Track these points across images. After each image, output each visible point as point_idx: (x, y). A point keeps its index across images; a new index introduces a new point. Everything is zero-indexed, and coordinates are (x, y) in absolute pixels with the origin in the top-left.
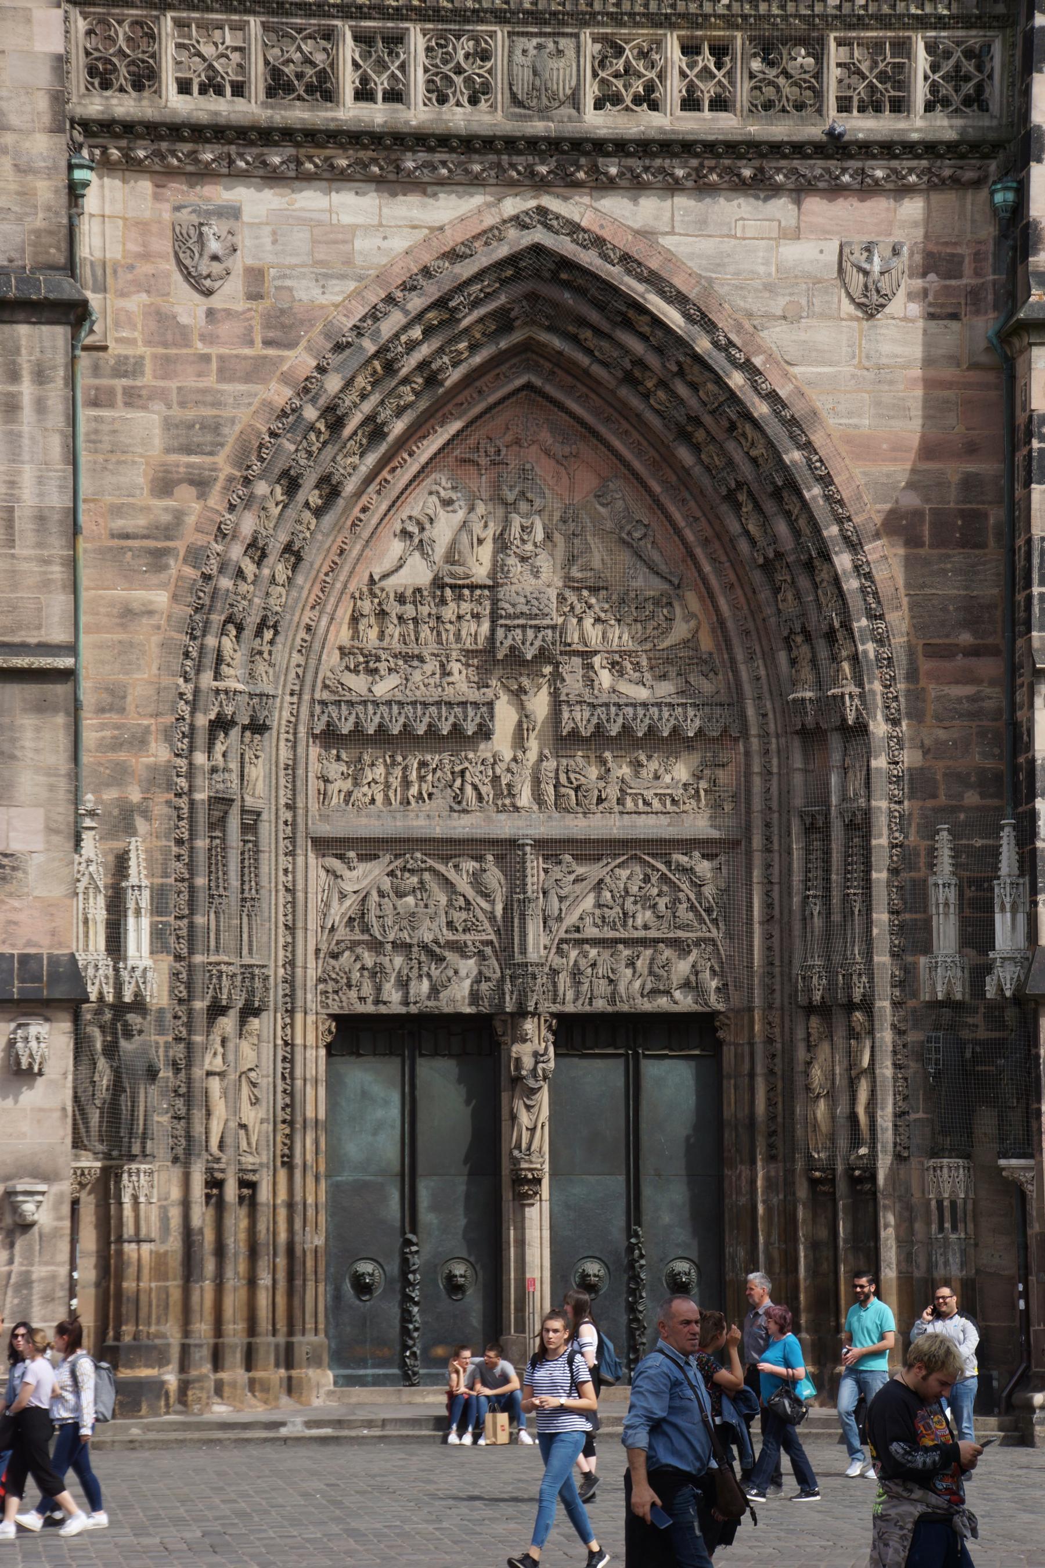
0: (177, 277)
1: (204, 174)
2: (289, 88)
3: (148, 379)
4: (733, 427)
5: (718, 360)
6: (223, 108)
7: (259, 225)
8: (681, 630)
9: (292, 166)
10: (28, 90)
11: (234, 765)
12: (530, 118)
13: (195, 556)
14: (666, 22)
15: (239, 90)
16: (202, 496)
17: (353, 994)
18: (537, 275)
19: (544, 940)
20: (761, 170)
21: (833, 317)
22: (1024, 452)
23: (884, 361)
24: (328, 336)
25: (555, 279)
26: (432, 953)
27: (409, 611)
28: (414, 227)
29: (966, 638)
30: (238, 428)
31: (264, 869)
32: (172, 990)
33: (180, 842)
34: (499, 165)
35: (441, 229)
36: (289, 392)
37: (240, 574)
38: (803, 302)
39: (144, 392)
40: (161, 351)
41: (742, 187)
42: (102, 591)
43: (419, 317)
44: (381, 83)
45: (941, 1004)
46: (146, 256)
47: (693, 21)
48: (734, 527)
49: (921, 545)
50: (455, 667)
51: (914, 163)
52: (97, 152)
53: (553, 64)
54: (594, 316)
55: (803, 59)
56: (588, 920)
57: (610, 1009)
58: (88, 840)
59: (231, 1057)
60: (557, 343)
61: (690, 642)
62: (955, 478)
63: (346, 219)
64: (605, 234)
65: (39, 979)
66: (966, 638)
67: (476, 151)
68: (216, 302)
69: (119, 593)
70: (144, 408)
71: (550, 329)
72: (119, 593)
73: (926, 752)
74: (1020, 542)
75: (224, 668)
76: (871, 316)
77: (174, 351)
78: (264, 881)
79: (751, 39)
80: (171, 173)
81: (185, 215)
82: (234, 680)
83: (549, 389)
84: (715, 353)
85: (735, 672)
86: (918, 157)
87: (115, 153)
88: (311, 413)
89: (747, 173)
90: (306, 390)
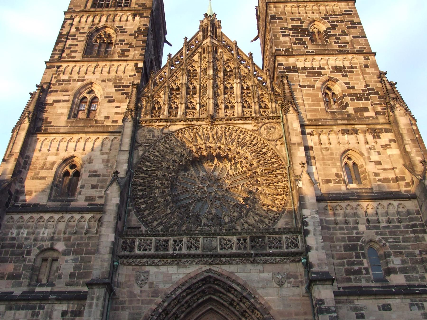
0: (135, 285)
2: (160, 249)
3: (127, 305)
4: (253, 312)
5: (248, 297)
7: (153, 274)
10: (106, 247)
20: (255, 259)
21: (271, 287)
30: (144, 314)
34: (201, 260)
35: (190, 273)
36: (156, 306)
44: (177, 248)
46: (129, 281)
51: (285, 257)
63: (170, 272)
64: (224, 273)
67: (197, 258)
68: (143, 289)
70: (125, 310)
71: (214, 295)
80: (136, 265)
83: (215, 309)
86: (286, 256)
88: (160, 310)
89: (252, 260)
90: (159, 306)
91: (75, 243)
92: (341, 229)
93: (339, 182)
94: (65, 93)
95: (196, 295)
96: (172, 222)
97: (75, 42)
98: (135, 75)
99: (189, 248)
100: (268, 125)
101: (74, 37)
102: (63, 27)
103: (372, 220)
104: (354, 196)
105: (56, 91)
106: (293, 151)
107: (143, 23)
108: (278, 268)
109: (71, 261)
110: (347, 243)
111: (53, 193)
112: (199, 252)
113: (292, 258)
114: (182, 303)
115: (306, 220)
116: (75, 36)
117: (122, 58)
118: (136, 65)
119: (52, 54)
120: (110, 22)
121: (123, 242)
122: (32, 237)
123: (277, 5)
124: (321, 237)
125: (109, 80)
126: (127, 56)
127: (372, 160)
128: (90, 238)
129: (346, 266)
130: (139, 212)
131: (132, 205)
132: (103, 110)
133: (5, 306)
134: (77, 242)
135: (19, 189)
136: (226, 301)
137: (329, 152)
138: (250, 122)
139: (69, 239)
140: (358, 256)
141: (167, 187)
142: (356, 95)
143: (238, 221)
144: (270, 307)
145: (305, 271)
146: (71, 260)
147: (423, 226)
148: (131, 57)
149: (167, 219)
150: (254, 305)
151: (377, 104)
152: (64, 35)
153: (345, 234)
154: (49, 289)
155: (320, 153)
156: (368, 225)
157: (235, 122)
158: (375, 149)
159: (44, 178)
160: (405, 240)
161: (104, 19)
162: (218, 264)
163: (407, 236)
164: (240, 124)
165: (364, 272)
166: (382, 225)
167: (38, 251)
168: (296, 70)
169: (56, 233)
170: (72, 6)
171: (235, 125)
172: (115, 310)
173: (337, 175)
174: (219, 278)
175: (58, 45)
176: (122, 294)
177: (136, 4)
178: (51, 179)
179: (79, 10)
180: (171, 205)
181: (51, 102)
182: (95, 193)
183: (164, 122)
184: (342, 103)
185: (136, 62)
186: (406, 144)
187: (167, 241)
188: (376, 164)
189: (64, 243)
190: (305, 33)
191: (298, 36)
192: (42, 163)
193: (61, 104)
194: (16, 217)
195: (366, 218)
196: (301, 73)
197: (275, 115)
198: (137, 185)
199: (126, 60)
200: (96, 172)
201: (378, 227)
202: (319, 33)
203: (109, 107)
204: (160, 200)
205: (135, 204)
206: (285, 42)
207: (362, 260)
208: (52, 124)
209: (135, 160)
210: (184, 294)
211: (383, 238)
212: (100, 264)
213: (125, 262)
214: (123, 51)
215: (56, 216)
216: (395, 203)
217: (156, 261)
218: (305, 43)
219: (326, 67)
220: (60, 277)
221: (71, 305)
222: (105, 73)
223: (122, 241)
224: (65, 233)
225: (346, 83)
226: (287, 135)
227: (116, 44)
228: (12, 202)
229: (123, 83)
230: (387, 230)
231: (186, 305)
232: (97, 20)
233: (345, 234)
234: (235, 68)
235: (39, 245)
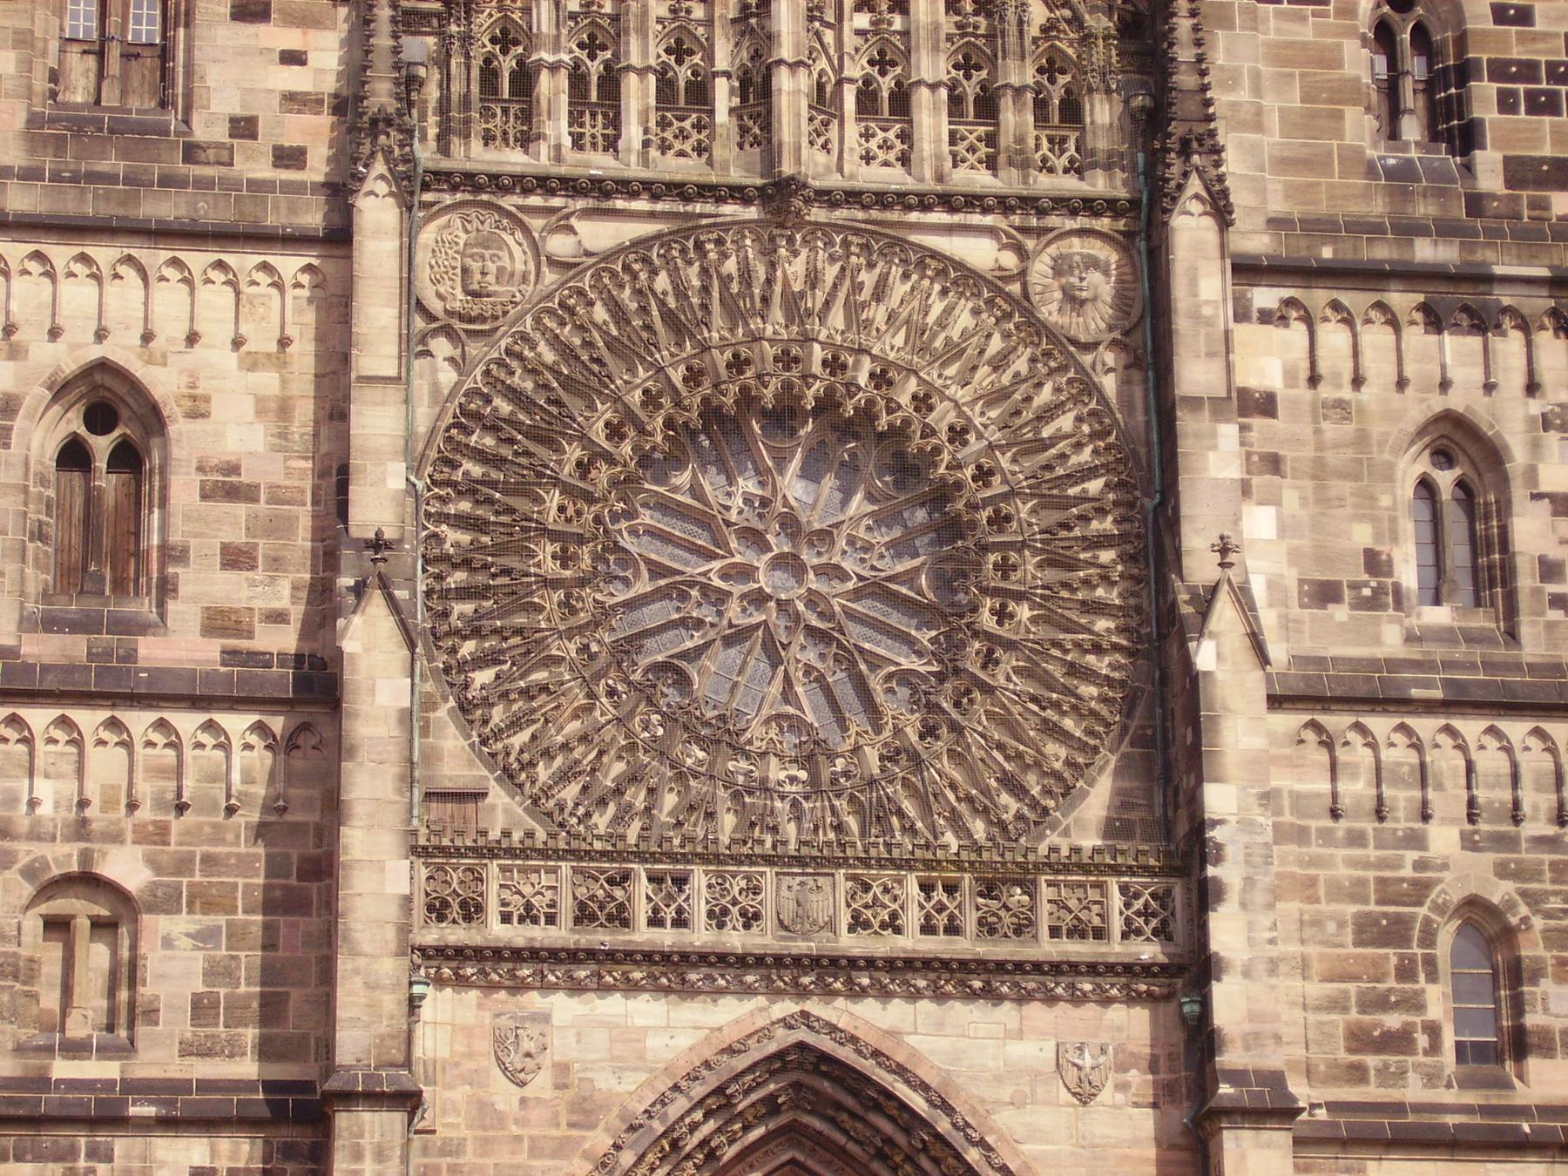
0: (497, 1071)
1: (518, 987)
2: (593, 917)
5: (957, 1139)
6: (541, 935)
7: (566, 1027)
9: (595, 979)
12: (795, 940)
14: (908, 864)
15: (551, 919)
18: (800, 1066)
20: (988, 983)
23: (1097, 1141)
24: (622, 1118)
25: (816, 1071)
28: (697, 1028)
34: (769, 978)
35: (720, 1029)
38: (1028, 1090)
39: (465, 1169)
40: (481, 1133)
43: (701, 1102)
44: (669, 914)
46: (470, 1055)
47: (929, 865)
51: (1115, 980)
52: (432, 971)
53: (813, 897)
54: (849, 1101)
55: (1018, 896)
60: (817, 1124)
63: (639, 1022)
68: (528, 1091)
71: (811, 1112)
76: (1085, 1103)
77: (491, 1133)
79: (977, 880)
80: (493, 987)
81: (503, 1021)
83: (811, 1163)
84: (954, 1132)
87: (446, 971)
89: (977, 984)
91: (193, 854)
92: (1356, 839)
93: (1373, 603)
96: (619, 768)
99: (718, 917)
100: (1076, 245)
103: (1491, 802)
104: (1428, 685)
109: (188, 942)
110: (1372, 907)
127: (1544, 488)
129: (1354, 1015)
131: (434, 671)
134: (199, 850)
136: (857, 1142)
137: (1349, 428)
138: (989, 220)
139: (160, 834)
140: (1406, 972)
142: (1528, 70)
146: (188, 935)
149: (601, 753)
153: (1366, 864)
154: (110, 1070)
155: (1309, 430)
156: (1470, 827)
157: (914, 216)
165: (1422, 1040)
166: (1529, 829)
167: (28, 890)
169: (96, 801)
171: (914, 238)
174: (845, 1054)
182: (245, 593)
188: (1556, 513)
198: (444, 558)
200: (234, 469)
203: (243, 52)
205: (447, 670)
207: (1423, 991)
210: (698, 1115)
211: (1524, 894)
212: (363, 1000)
213: (446, 971)
215: (88, 719)
220: (152, 1015)
223: (424, 873)
230: (1547, 857)
233: (1366, 864)
235: (23, 860)
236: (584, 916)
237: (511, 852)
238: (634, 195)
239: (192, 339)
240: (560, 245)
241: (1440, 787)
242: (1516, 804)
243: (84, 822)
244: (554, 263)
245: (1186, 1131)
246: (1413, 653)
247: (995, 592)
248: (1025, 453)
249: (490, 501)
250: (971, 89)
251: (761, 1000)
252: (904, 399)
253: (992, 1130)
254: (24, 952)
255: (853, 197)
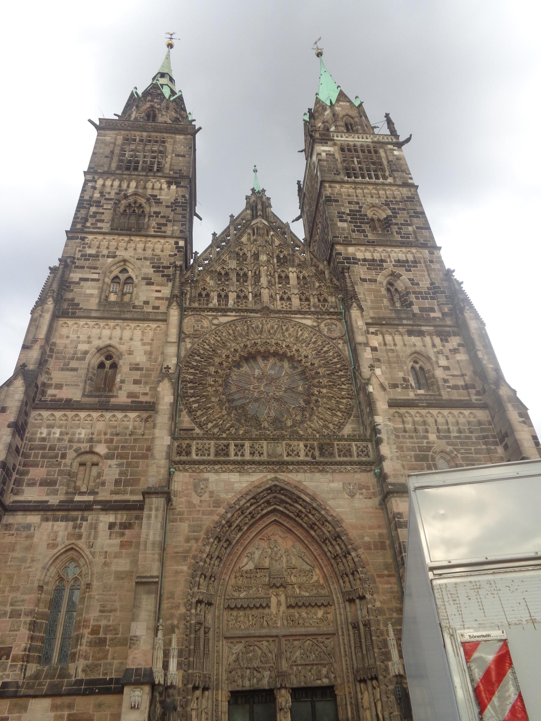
0: (194, 493)
2: (220, 454)
3: (185, 516)
4: (323, 525)
5: (318, 508)
8: (315, 578)
11: (202, 613)
13: (194, 557)
16: (197, 542)
17: (235, 684)
19: (287, 665)
22: (394, 522)
24: (228, 505)
25: (280, 493)
26: (257, 669)
27: (249, 575)
29: (386, 572)
31: (210, 645)
32: (183, 681)
33: (187, 635)
36: (218, 517)
37: (205, 562)
41: (320, 471)
42: (171, 567)
43: (249, 501)
44: (239, 453)
45: (396, 676)
46: (187, 489)
48: (326, 550)
49: (371, 549)
50: (260, 589)
54: (289, 501)
56: (298, 659)
57: (305, 686)
58: (160, 634)
59: (199, 704)
61: (317, 581)
62: (377, 534)
65: (140, 675)
66: (386, 572)
68: (202, 498)
69: (175, 567)
71: (279, 505)
72: (175, 567)
73: (381, 602)
74: (397, 545)
75: (201, 587)
78: (210, 649)
80: (194, 472)
82: (203, 590)
83: (280, 520)
85: (330, 587)
88: (224, 522)
90: (223, 517)
92: (411, 437)
93: (406, 388)
94: (93, 271)
95: (260, 505)
96: (228, 425)
97: (101, 210)
98: (176, 255)
99: (252, 454)
100: (329, 321)
101: (98, 204)
102: (84, 190)
105: (82, 267)
106: (359, 351)
107: (180, 194)
108: (348, 477)
109: (115, 466)
111: (87, 387)
112: (264, 458)
113: (364, 467)
114: (246, 514)
115: (378, 427)
116: (100, 202)
117: (159, 234)
118: (176, 243)
119: (73, 222)
120: (141, 189)
121: (178, 446)
122: (67, 438)
123: (333, 185)
124: (395, 447)
125: (145, 259)
126: (165, 232)
128: (135, 440)
130: (190, 412)
131: (183, 404)
132: (140, 294)
133: (40, 516)
134: (120, 445)
135: (46, 381)
136: (292, 513)
138: (310, 316)
139: (111, 441)
141: (221, 385)
142: (421, 293)
143: (301, 426)
144: (342, 519)
145: (378, 482)
147: (495, 438)
148: (169, 233)
150: (325, 517)
151: (443, 304)
152: (86, 200)
154: (91, 498)
158: (443, 353)
159: (75, 370)
160: (477, 452)
161: (133, 184)
162: (284, 472)
163: (479, 447)
164: (298, 319)
166: (453, 435)
167: (75, 454)
168: (356, 261)
169: (96, 434)
170: (93, 165)
172: (173, 522)
173: (404, 379)
174: (286, 487)
175: (79, 211)
176: (179, 503)
177: (170, 170)
178: (85, 371)
179: (101, 171)
180: (227, 405)
181: (77, 280)
183: (213, 312)
184: (406, 301)
185: (176, 240)
186: (479, 350)
187: (227, 446)
189: (105, 445)
190: (364, 219)
191: (356, 222)
192: (72, 352)
193: (90, 283)
194: (45, 414)
195: (436, 427)
196: (362, 265)
197: (336, 310)
198: (186, 381)
199: (165, 237)
200: (139, 365)
201: (448, 437)
202: (379, 220)
203: (147, 290)
204: (213, 399)
205: (186, 403)
206: (343, 229)
208: (81, 306)
209: (183, 354)
211: (454, 449)
213: (181, 468)
214: (160, 225)
215: (95, 415)
216: (467, 412)
217: (216, 467)
218: (364, 231)
219: (388, 260)
220: (103, 484)
221: (119, 516)
222: (140, 251)
223: (176, 444)
224: (105, 434)
225: (409, 279)
226: (351, 334)
227: (150, 216)
228: (39, 396)
229: (163, 263)
231: (249, 516)
232: (124, 186)
233: (415, 443)
234: (289, 254)
235: (75, 447)
236: (217, 454)
237: (200, 439)
238: (232, 312)
239: (131, 339)
240: (215, 322)
241: (429, 426)
242: (449, 429)
243: (92, 438)
244: (213, 324)
245: (380, 504)
246: (417, 398)
247: (317, 387)
248: (322, 360)
249: (197, 370)
250: (303, 298)
251: (265, 474)
252: (294, 350)
253: (328, 505)
254: (73, 471)
255: (279, 312)
